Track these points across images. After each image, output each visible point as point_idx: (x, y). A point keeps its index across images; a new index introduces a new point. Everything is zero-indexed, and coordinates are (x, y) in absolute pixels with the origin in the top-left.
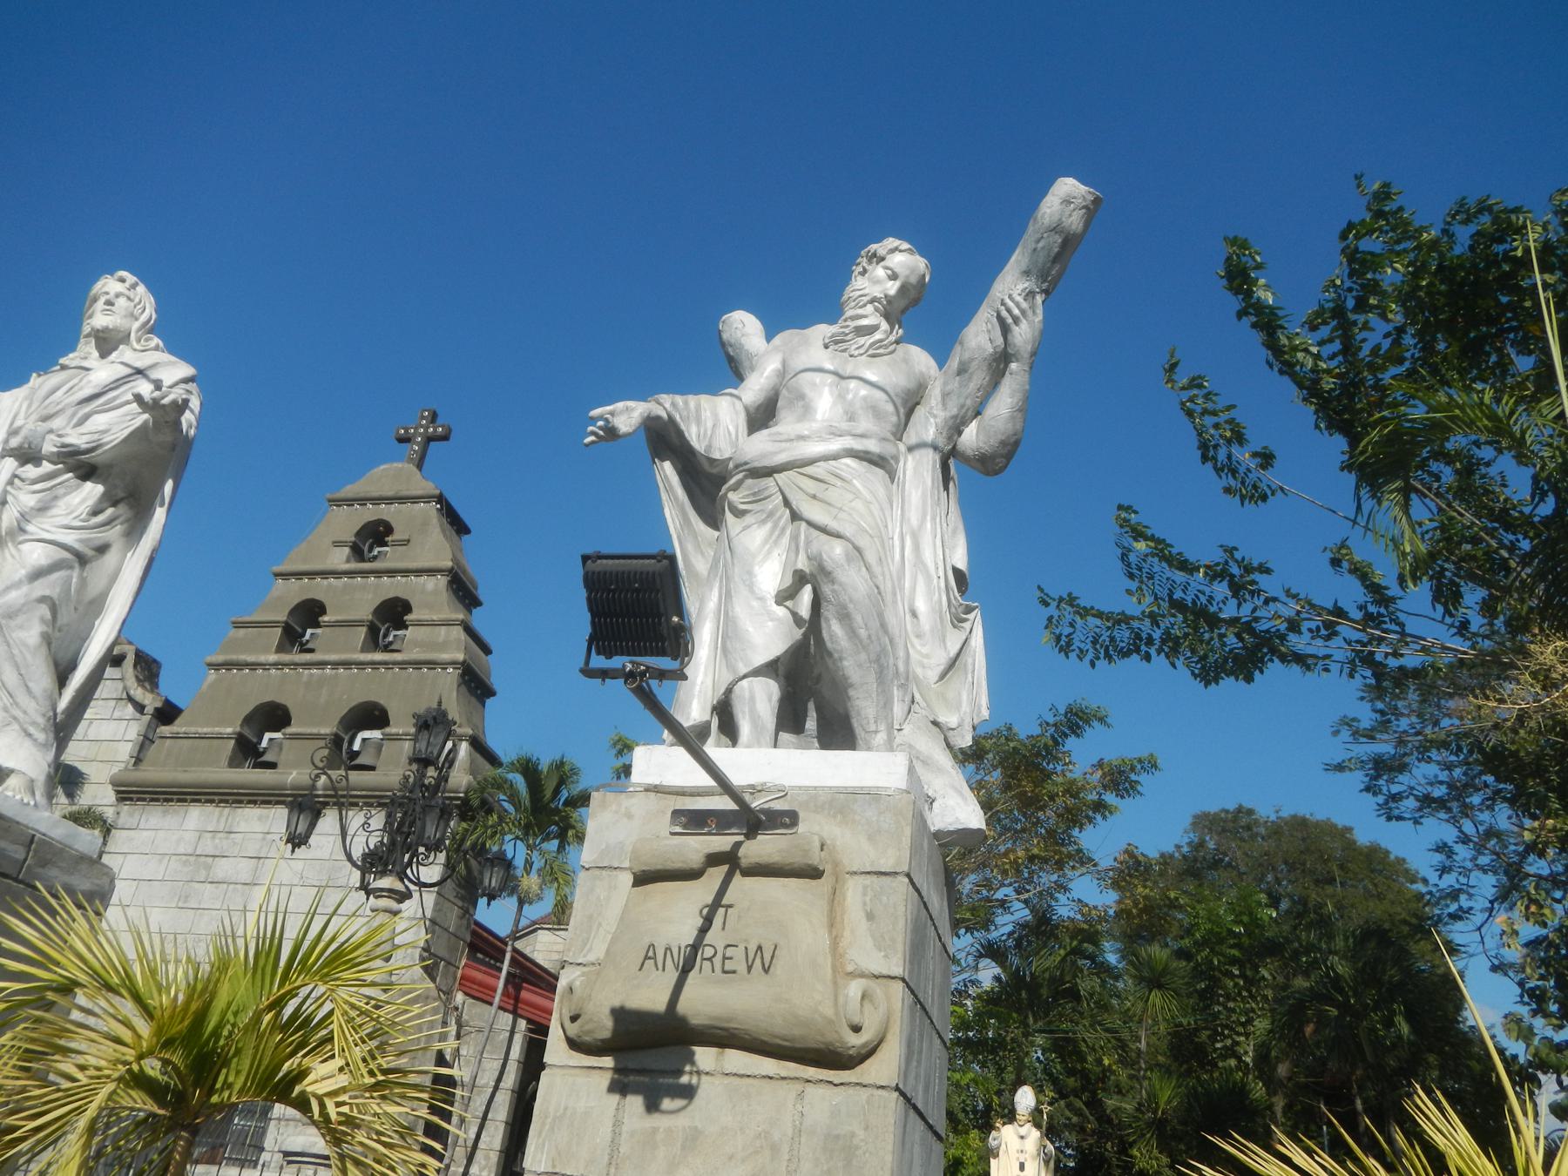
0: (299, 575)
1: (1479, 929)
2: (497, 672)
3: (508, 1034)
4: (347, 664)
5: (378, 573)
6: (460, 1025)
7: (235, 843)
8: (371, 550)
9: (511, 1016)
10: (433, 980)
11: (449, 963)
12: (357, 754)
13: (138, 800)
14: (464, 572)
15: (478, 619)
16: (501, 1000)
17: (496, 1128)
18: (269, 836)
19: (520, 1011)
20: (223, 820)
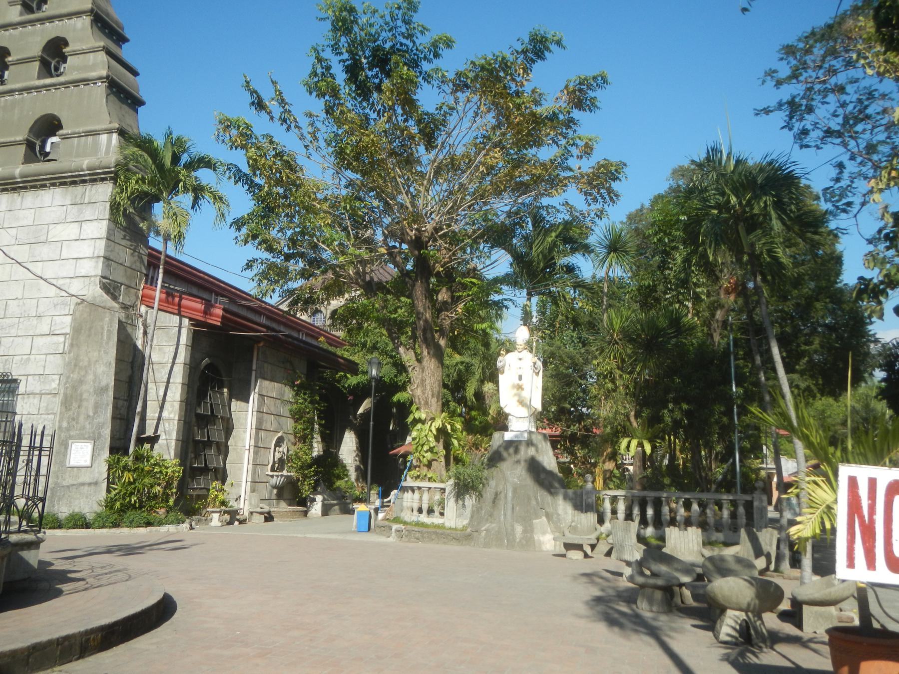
1: (855, 216)
2: (143, 87)
3: (177, 329)
4: (28, 89)
5: (42, 20)
6: (145, 326)
8: (39, 8)
9: (178, 317)
10: (115, 298)
11: (128, 287)
12: (48, 153)
14: (108, 15)
15: (126, 52)
16: (159, 305)
17: (176, 388)
19: (182, 313)
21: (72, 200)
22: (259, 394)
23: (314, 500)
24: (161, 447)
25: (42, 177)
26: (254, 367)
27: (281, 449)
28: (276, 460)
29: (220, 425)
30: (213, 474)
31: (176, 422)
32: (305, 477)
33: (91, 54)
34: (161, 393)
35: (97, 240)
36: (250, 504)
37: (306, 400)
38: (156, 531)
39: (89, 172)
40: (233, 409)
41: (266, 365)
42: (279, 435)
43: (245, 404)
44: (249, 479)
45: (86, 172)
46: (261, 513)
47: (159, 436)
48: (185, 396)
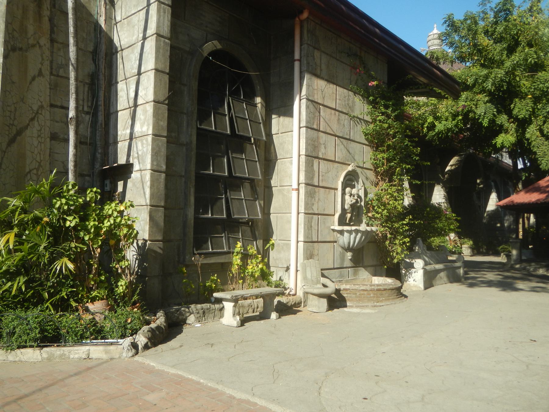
22: (308, 99)
23: (411, 266)
24: (134, 184)
26: (297, 56)
27: (354, 191)
28: (347, 207)
29: (253, 152)
30: (248, 229)
31: (150, 138)
32: (395, 233)
34: (132, 95)
36: (305, 278)
37: (388, 116)
38: (61, 356)
40: (274, 132)
41: (317, 54)
42: (350, 168)
43: (291, 119)
44: (301, 238)
46: (321, 296)
47: (132, 165)
48: (165, 93)
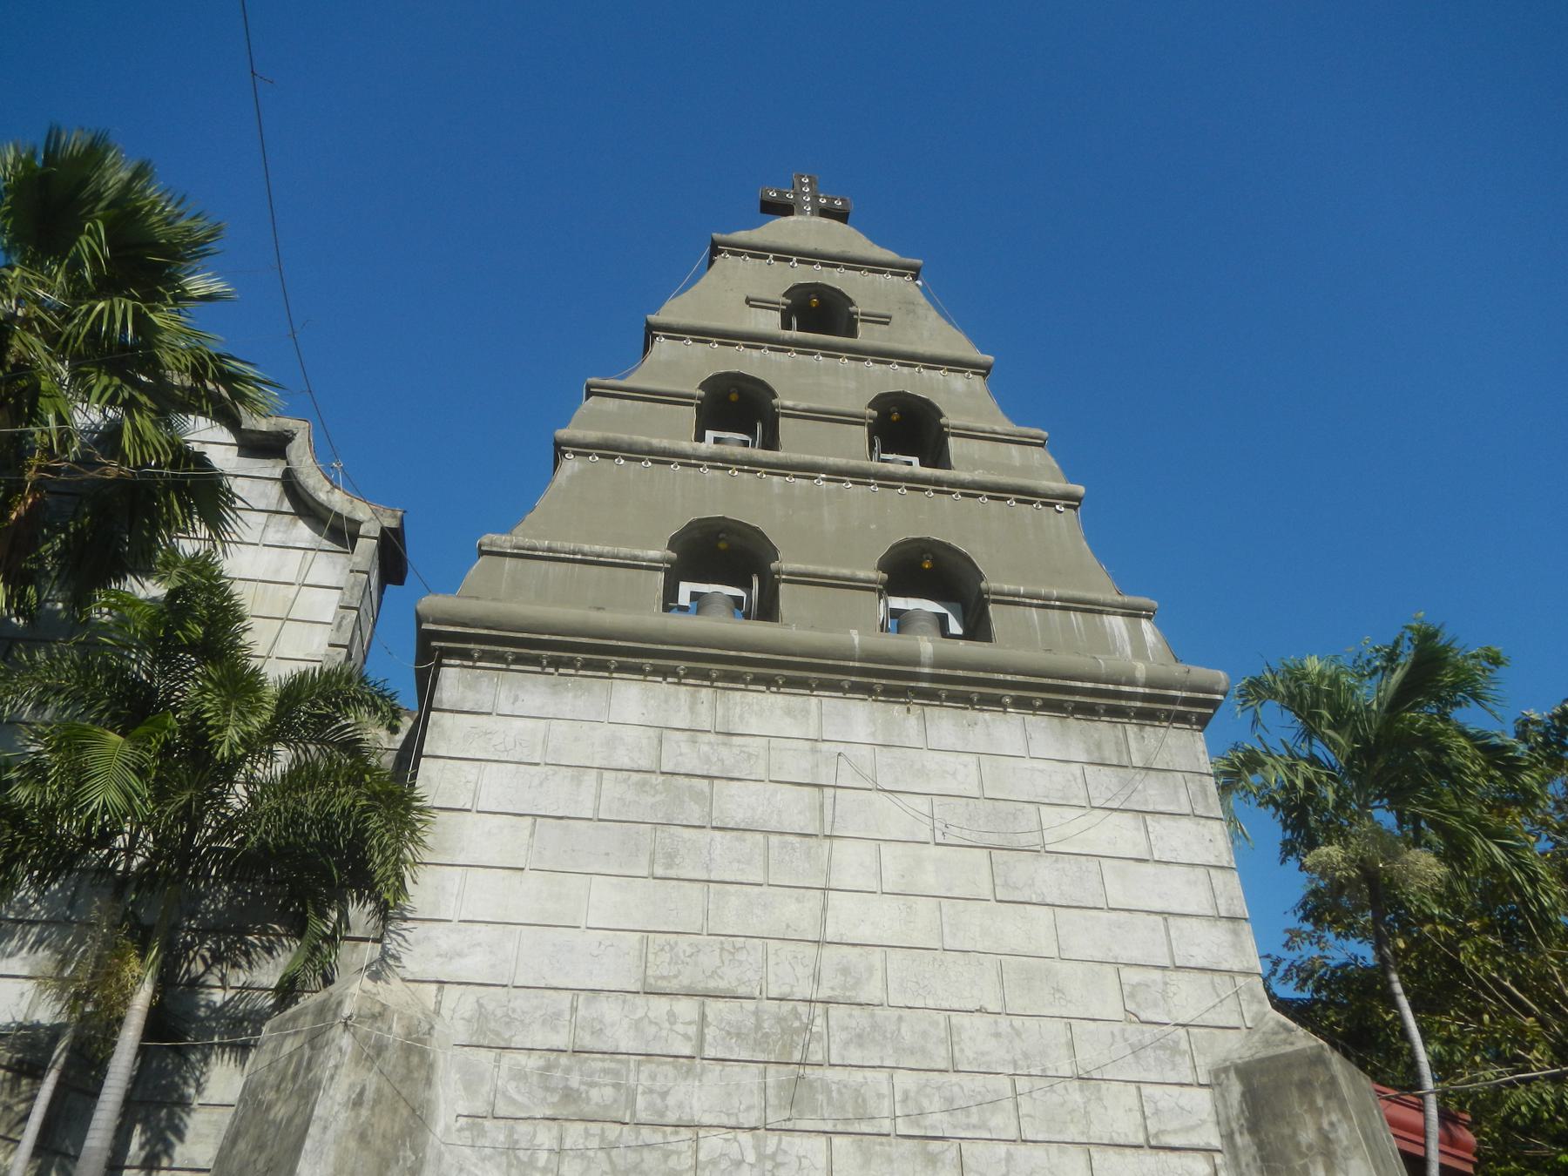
0: (702, 335)
5: (859, 354)
7: (750, 755)
13: (485, 656)
18: (820, 745)
20: (704, 709)
21: (1088, 752)
25: (1001, 677)
33: (1014, 448)
35: (1212, 871)
39: (1147, 690)
45: (1140, 690)
